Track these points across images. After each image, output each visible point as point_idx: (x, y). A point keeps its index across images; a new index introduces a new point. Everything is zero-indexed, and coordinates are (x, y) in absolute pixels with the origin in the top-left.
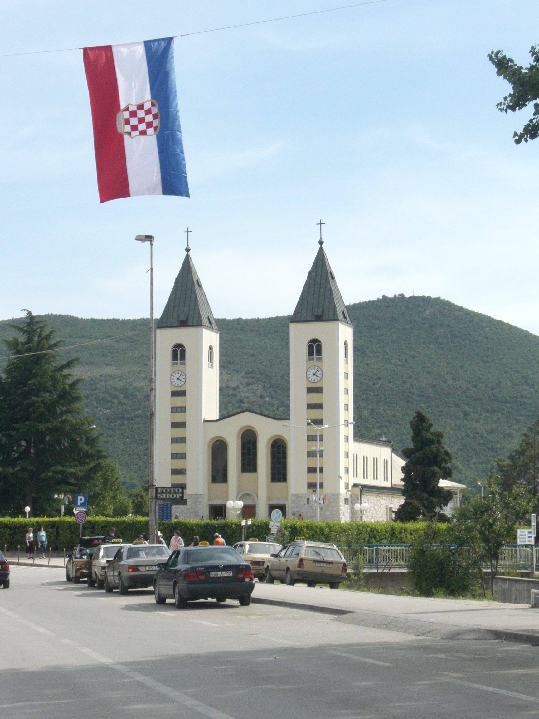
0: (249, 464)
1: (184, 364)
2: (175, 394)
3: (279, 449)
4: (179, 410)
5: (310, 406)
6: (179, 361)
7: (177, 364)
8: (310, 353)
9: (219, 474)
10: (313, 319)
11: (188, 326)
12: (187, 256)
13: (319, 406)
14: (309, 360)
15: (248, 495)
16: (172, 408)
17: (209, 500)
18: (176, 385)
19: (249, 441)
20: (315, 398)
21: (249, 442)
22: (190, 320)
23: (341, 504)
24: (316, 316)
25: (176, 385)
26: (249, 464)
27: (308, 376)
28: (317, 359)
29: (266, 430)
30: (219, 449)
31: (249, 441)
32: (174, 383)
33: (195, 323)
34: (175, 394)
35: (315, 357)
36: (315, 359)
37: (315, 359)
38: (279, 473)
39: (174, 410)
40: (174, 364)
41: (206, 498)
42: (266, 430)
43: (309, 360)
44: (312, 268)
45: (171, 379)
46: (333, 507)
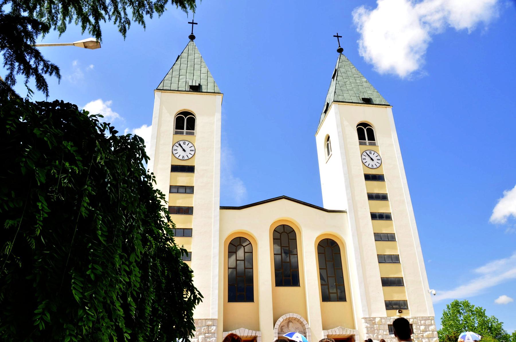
3: (330, 252)
4: (181, 190)
6: (185, 131)
7: (182, 133)
8: (361, 137)
11: (202, 92)
16: (171, 187)
18: (181, 158)
19: (285, 238)
25: (181, 158)
27: (364, 161)
28: (370, 144)
31: (285, 238)
32: (177, 156)
36: (367, 144)
37: (367, 144)
38: (334, 287)
39: (176, 190)
43: (361, 144)
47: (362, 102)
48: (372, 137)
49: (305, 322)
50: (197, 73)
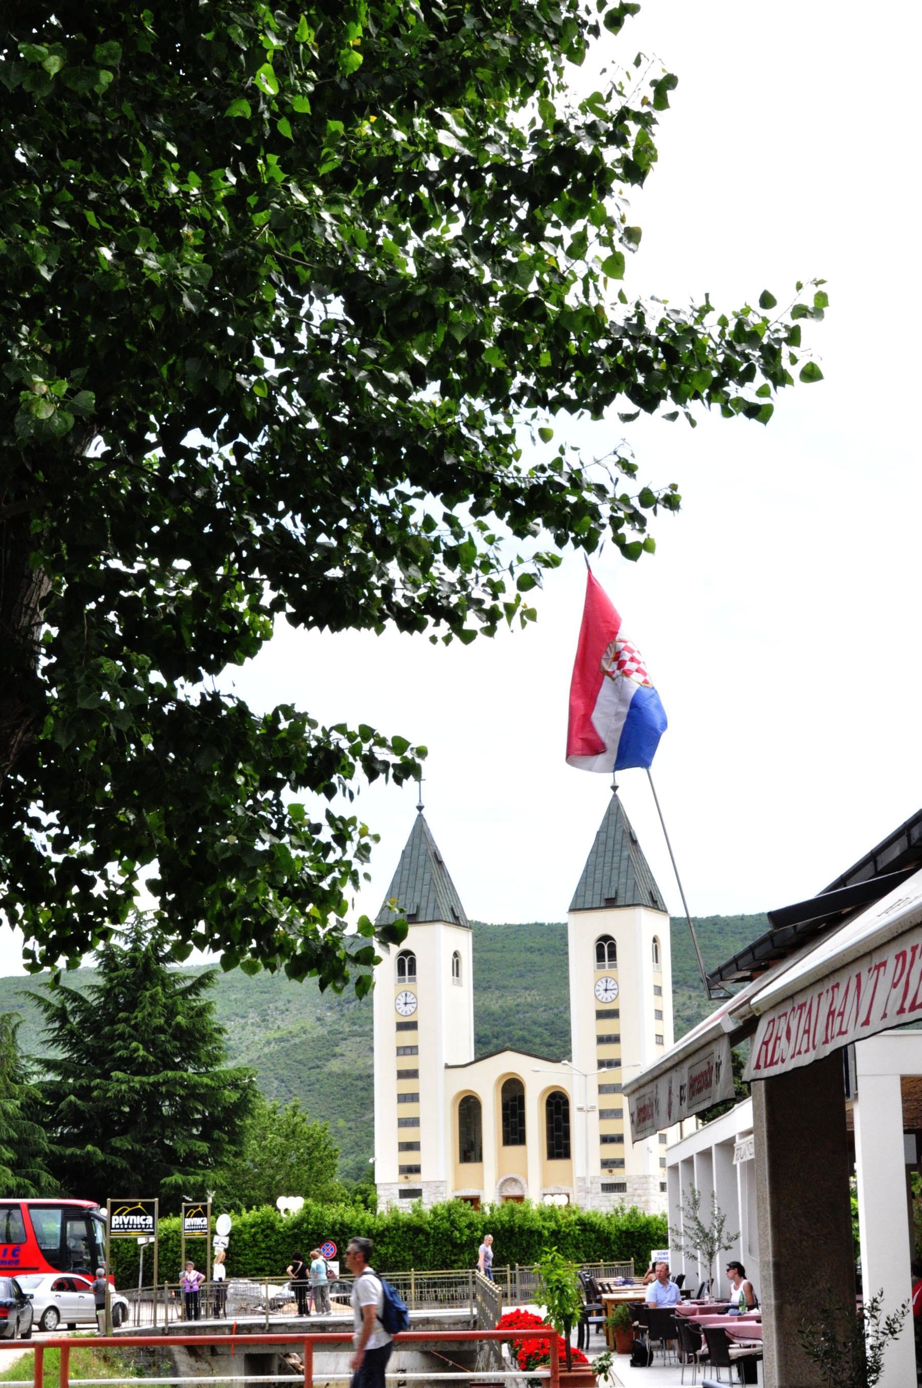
0: (514, 1133)
1: (414, 980)
2: (403, 1026)
3: (558, 1106)
4: (408, 1051)
5: (601, 1040)
6: (407, 976)
7: (404, 981)
8: (600, 957)
9: (470, 1150)
10: (603, 905)
12: (420, 816)
13: (614, 1039)
14: (599, 967)
15: (514, 1180)
16: (398, 1048)
17: (456, 1189)
19: (513, 1095)
20: (608, 1027)
21: (514, 1099)
22: (422, 913)
23: (652, 1191)
24: (607, 900)
26: (514, 1133)
28: (610, 966)
29: (538, 1077)
30: (469, 1109)
31: (513, 1095)
33: (429, 918)
34: (403, 1026)
35: (607, 963)
38: (559, 1145)
39: (401, 1052)
40: (399, 981)
41: (450, 1186)
42: (538, 1077)
43: (599, 967)
44: (602, 827)
45: (396, 1004)
46: (640, 1196)
47: (603, 905)
48: (613, 955)
49: (523, 1182)
50: (417, 894)
